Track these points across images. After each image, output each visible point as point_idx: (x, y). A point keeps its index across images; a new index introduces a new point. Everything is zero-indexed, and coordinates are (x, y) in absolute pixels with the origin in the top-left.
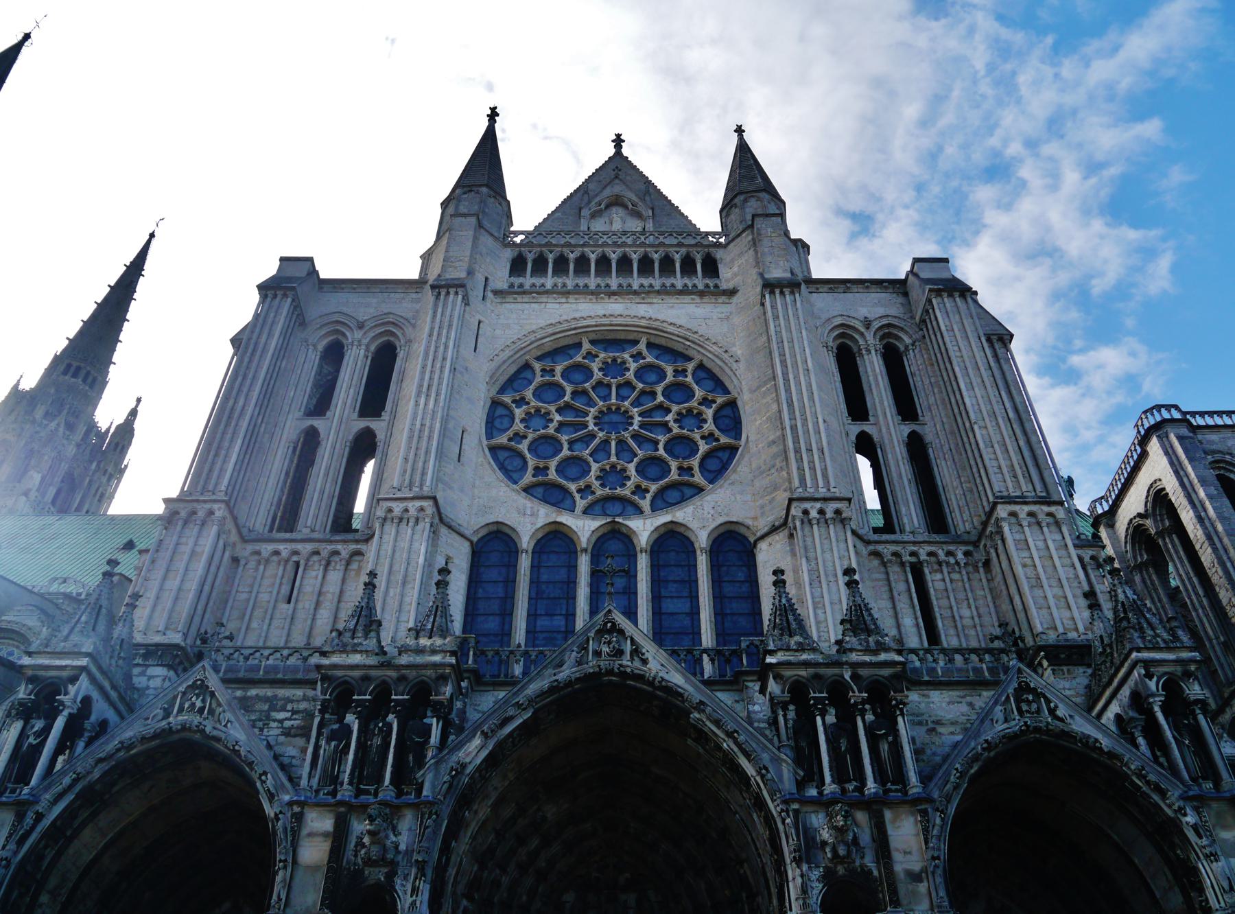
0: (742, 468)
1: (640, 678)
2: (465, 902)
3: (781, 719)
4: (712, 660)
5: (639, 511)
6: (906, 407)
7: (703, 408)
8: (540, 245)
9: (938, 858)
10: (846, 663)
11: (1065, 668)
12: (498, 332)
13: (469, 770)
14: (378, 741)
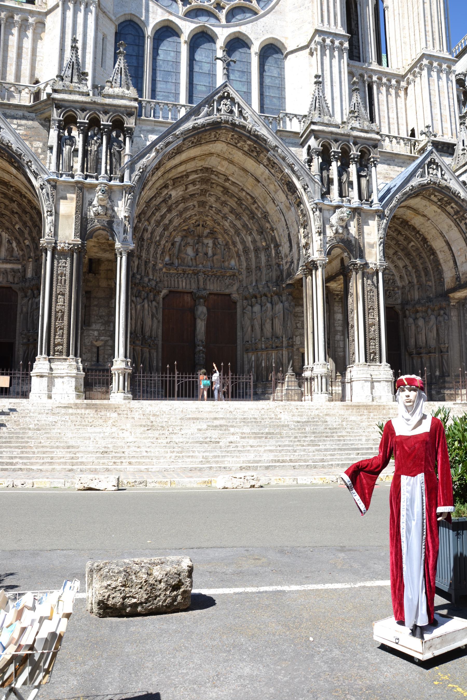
1: (244, 127)
14: (94, 148)
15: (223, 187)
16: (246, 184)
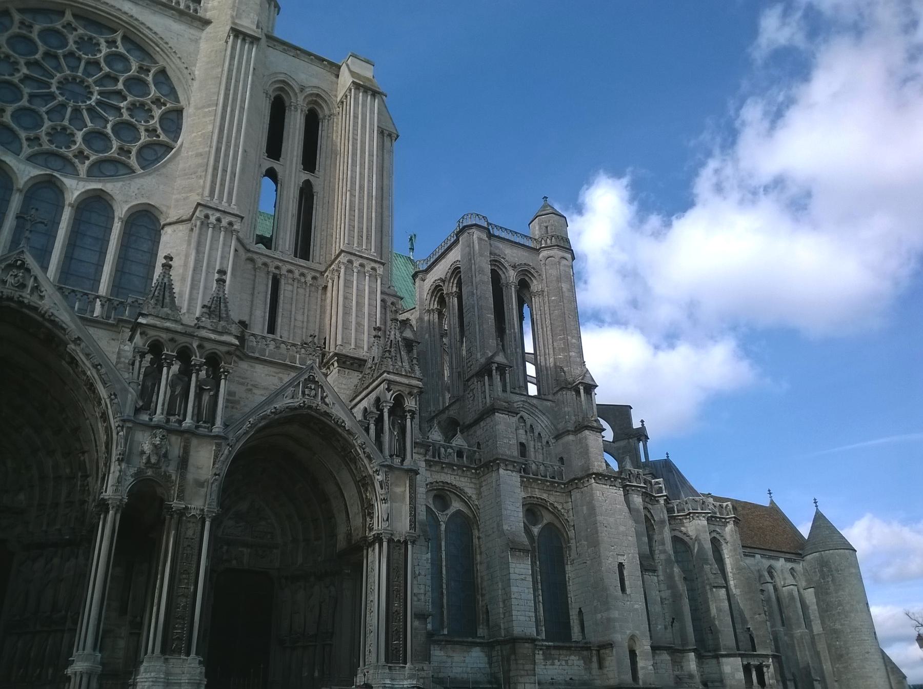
1: (35, 309)
3: (137, 364)
4: (102, 305)
5: (75, 174)
6: (309, 161)
7: (154, 107)
9: (219, 475)
10: (197, 336)
11: (347, 371)
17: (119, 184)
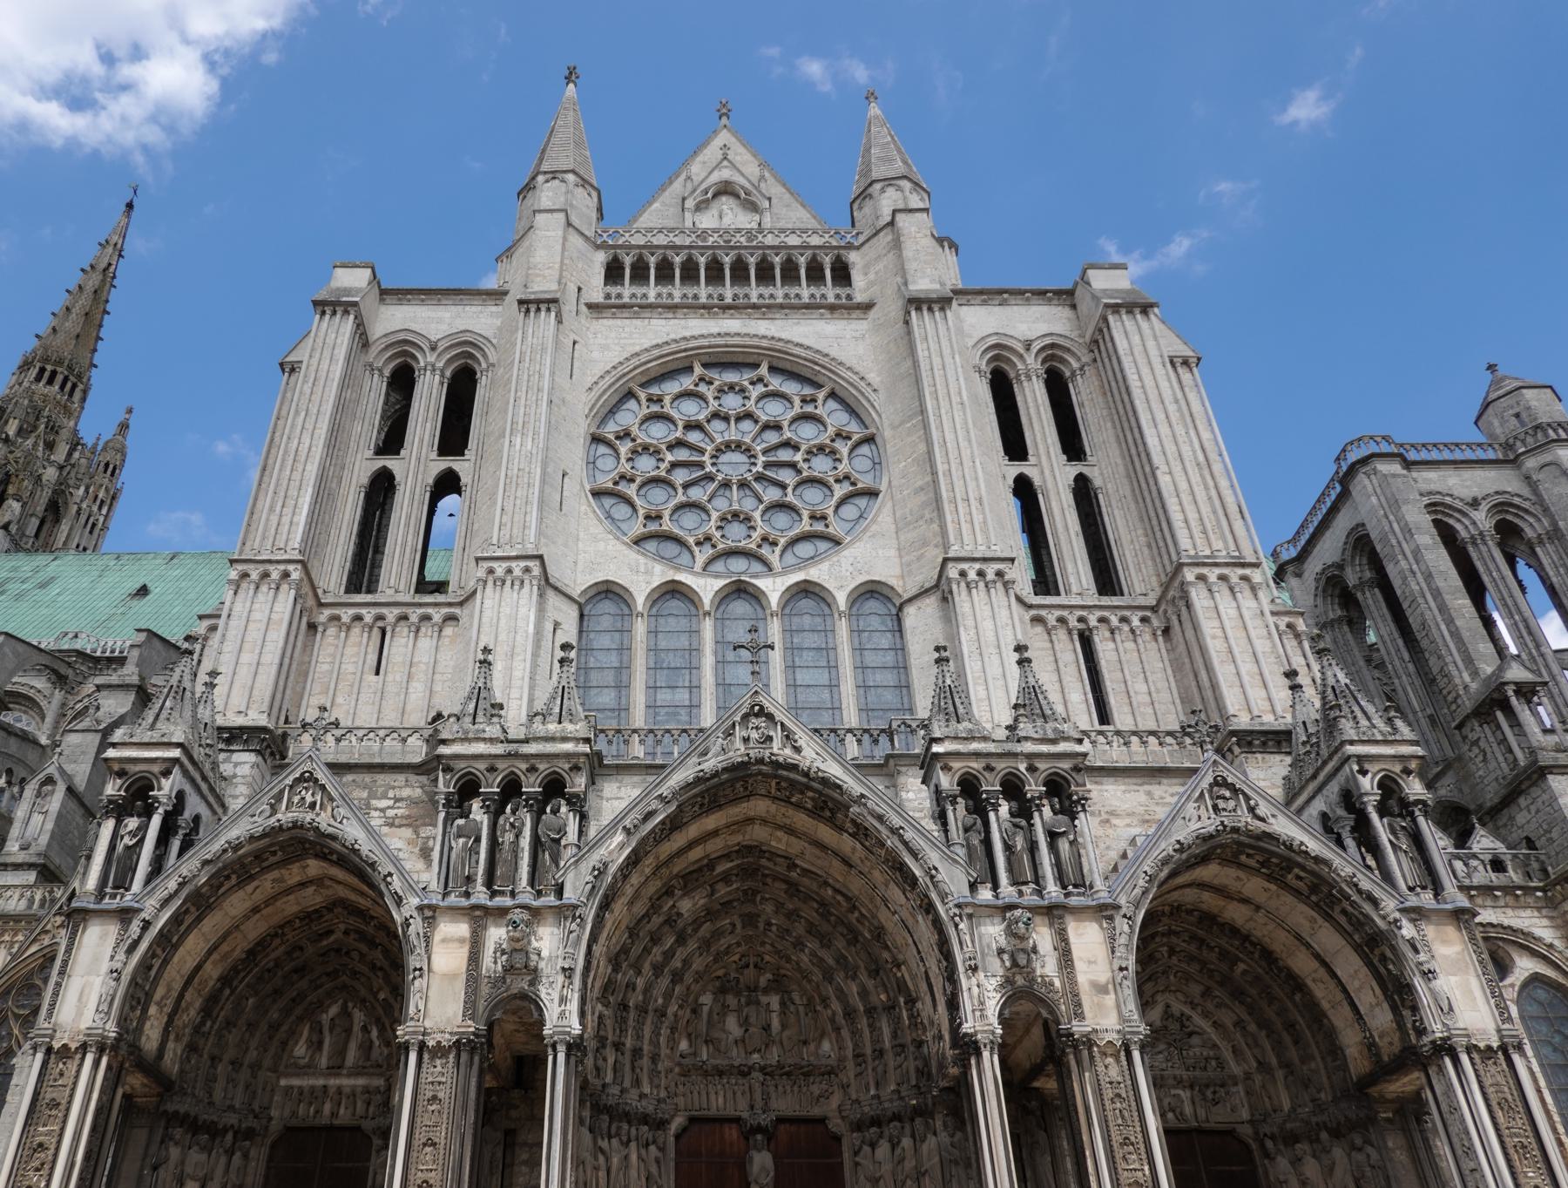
0: (883, 515)
1: (794, 767)
2: (599, 1007)
4: (859, 741)
8: (639, 247)
12: (596, 355)
13: (613, 869)
14: (509, 837)
15: (786, 882)
16: (831, 871)
17: (825, 566)
